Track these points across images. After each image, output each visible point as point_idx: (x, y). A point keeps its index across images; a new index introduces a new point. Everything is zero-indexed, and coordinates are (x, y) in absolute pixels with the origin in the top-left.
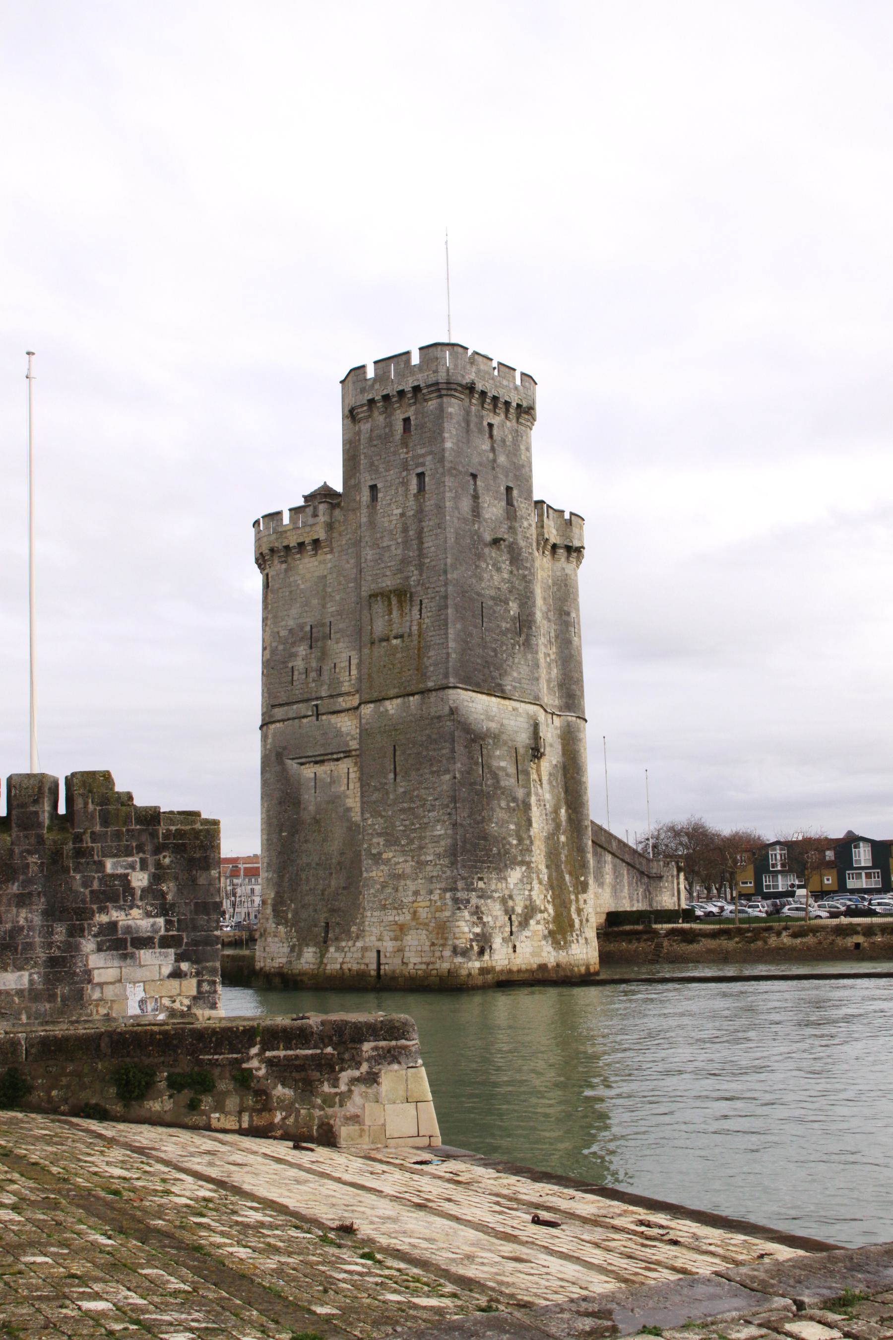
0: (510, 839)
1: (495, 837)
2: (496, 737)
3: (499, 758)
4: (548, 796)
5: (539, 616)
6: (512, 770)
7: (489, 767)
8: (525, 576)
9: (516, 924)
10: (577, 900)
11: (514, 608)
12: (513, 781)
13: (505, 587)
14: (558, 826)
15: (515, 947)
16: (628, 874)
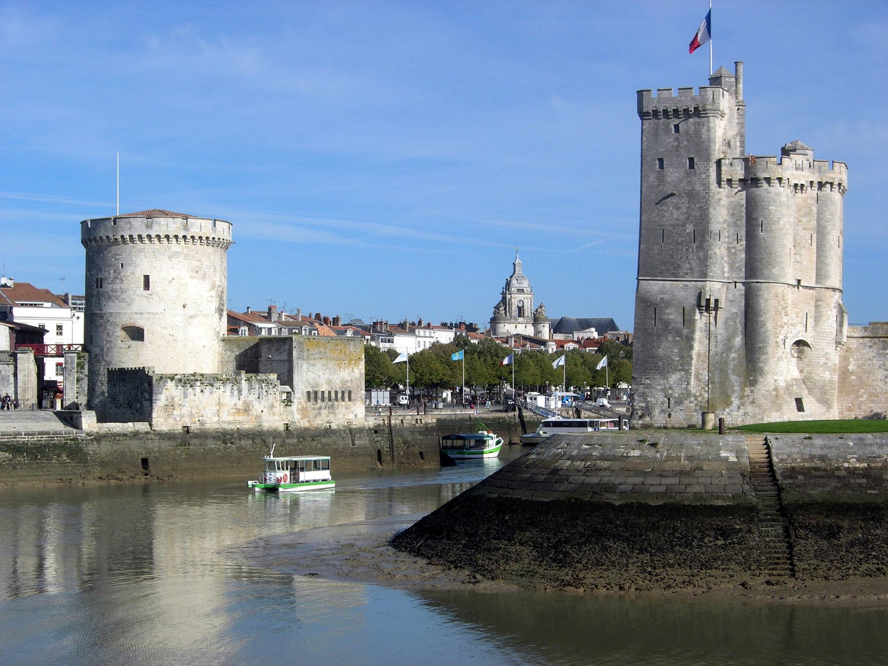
0: (673, 357)
1: (661, 357)
2: (668, 304)
3: (669, 314)
4: (722, 331)
5: (715, 227)
6: (681, 319)
7: (661, 319)
8: (700, 208)
9: (672, 402)
10: (743, 390)
11: (690, 228)
12: (680, 325)
13: (682, 217)
14: (729, 348)
15: (670, 415)
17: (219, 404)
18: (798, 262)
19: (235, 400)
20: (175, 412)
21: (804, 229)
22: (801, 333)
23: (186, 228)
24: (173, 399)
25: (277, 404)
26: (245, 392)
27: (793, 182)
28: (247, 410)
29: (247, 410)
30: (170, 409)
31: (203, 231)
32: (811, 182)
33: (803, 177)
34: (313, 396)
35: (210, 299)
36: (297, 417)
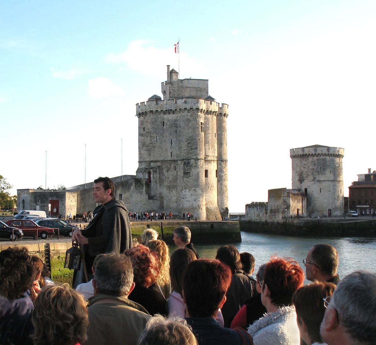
17: (254, 213)
28: (259, 216)
34: (272, 211)
35: (295, 177)
36: (268, 218)
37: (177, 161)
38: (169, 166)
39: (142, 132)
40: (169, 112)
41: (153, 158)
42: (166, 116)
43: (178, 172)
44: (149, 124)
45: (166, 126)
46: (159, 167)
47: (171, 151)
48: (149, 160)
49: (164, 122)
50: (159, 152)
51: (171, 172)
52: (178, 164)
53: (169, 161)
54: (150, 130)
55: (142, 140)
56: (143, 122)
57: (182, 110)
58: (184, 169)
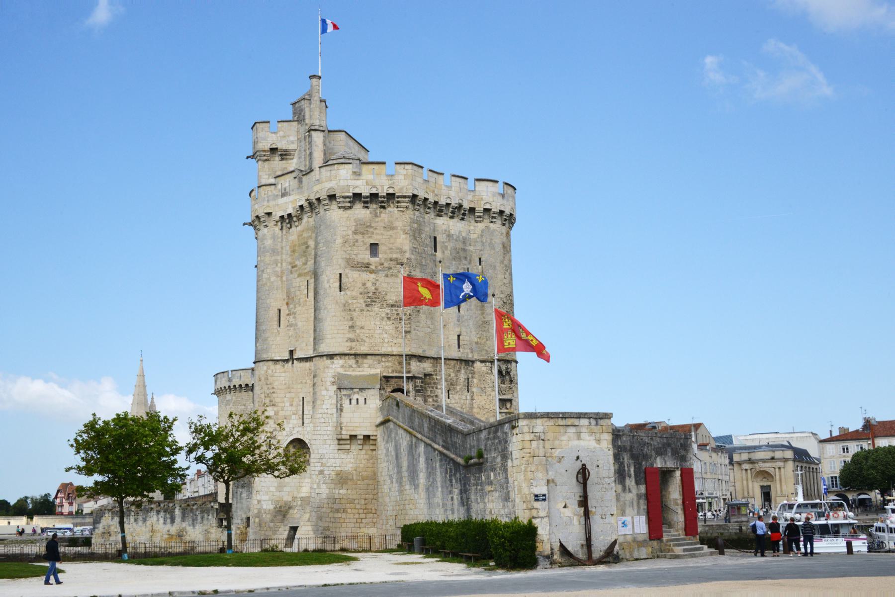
16: (441, 466)
17: (153, 531)
18: (291, 325)
19: (168, 526)
20: (111, 538)
21: (300, 275)
22: (296, 429)
23: (230, 380)
24: (109, 526)
25: (213, 530)
26: (178, 519)
27: (277, 214)
28: (180, 536)
29: (180, 536)
30: (106, 536)
31: (243, 379)
32: (301, 207)
33: (288, 205)
37: (473, 362)
38: (453, 375)
39: (364, 256)
40: (453, 213)
41: (415, 346)
42: (443, 223)
43: (475, 397)
44: (403, 236)
45: (443, 252)
46: (426, 375)
47: (457, 330)
48: (400, 349)
49: (435, 238)
50: (429, 330)
51: (457, 397)
52: (474, 373)
53: (453, 362)
54: (407, 255)
55: (364, 284)
56: (370, 226)
57: (494, 213)
58: (500, 392)
